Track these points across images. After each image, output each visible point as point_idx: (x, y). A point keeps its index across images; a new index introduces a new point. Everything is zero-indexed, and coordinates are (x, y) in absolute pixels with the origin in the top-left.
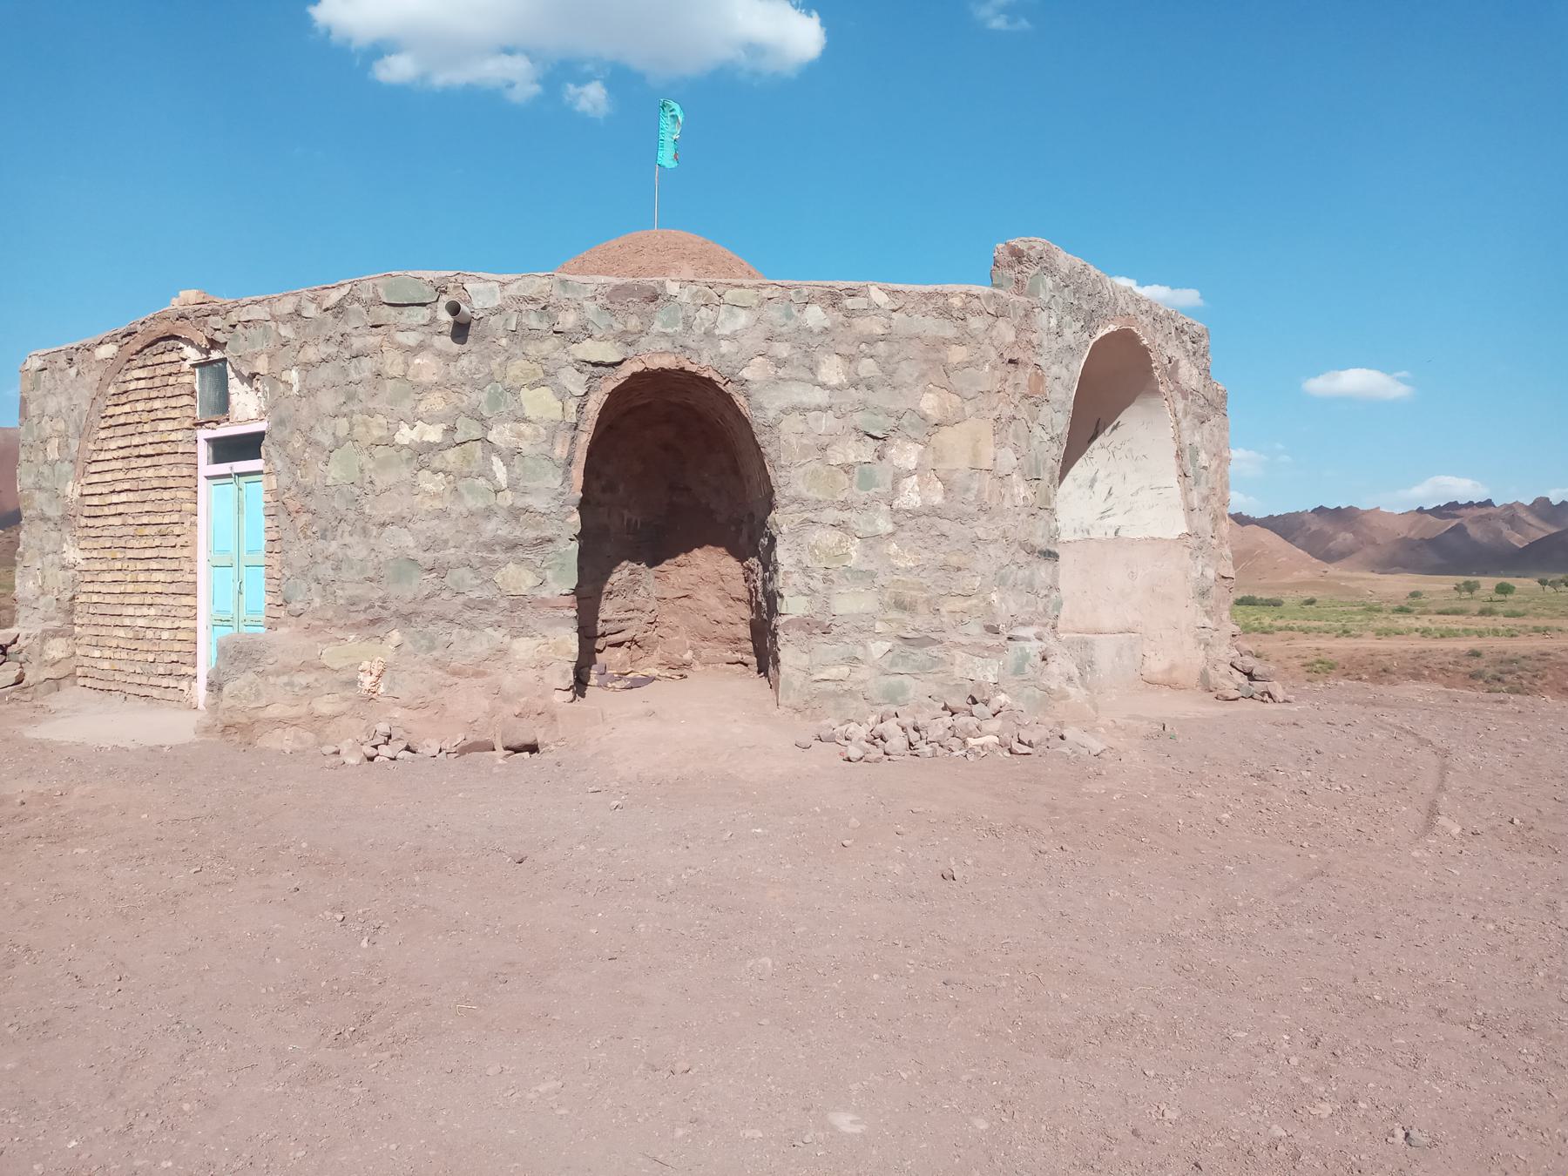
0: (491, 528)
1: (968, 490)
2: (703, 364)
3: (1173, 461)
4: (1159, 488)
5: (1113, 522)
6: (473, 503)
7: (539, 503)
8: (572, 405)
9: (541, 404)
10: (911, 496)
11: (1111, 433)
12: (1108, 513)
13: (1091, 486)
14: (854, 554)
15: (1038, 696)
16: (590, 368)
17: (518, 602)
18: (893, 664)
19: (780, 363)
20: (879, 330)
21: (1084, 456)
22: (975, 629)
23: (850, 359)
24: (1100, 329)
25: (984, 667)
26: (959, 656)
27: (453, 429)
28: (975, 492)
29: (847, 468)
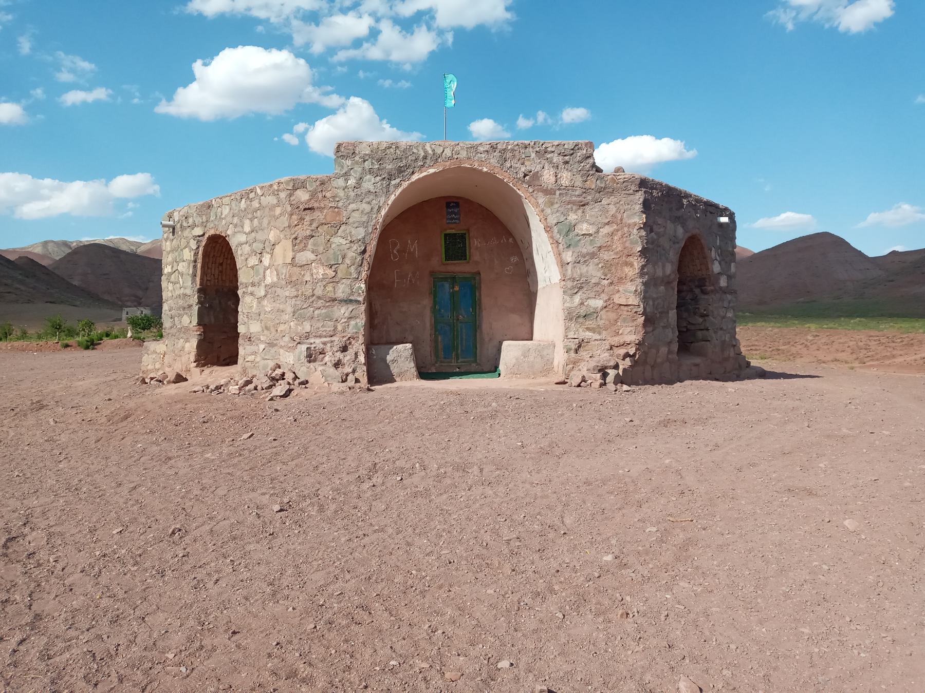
0: (181, 302)
1: (282, 274)
2: (220, 231)
6: (177, 293)
7: (188, 292)
8: (192, 253)
9: (188, 255)
10: (269, 280)
14: (255, 306)
15: (305, 371)
16: (198, 238)
17: (186, 329)
18: (265, 355)
19: (236, 226)
20: (258, 206)
22: (287, 339)
23: (251, 220)
25: (289, 356)
26: (282, 351)
27: (173, 267)
28: (284, 275)
29: (252, 267)
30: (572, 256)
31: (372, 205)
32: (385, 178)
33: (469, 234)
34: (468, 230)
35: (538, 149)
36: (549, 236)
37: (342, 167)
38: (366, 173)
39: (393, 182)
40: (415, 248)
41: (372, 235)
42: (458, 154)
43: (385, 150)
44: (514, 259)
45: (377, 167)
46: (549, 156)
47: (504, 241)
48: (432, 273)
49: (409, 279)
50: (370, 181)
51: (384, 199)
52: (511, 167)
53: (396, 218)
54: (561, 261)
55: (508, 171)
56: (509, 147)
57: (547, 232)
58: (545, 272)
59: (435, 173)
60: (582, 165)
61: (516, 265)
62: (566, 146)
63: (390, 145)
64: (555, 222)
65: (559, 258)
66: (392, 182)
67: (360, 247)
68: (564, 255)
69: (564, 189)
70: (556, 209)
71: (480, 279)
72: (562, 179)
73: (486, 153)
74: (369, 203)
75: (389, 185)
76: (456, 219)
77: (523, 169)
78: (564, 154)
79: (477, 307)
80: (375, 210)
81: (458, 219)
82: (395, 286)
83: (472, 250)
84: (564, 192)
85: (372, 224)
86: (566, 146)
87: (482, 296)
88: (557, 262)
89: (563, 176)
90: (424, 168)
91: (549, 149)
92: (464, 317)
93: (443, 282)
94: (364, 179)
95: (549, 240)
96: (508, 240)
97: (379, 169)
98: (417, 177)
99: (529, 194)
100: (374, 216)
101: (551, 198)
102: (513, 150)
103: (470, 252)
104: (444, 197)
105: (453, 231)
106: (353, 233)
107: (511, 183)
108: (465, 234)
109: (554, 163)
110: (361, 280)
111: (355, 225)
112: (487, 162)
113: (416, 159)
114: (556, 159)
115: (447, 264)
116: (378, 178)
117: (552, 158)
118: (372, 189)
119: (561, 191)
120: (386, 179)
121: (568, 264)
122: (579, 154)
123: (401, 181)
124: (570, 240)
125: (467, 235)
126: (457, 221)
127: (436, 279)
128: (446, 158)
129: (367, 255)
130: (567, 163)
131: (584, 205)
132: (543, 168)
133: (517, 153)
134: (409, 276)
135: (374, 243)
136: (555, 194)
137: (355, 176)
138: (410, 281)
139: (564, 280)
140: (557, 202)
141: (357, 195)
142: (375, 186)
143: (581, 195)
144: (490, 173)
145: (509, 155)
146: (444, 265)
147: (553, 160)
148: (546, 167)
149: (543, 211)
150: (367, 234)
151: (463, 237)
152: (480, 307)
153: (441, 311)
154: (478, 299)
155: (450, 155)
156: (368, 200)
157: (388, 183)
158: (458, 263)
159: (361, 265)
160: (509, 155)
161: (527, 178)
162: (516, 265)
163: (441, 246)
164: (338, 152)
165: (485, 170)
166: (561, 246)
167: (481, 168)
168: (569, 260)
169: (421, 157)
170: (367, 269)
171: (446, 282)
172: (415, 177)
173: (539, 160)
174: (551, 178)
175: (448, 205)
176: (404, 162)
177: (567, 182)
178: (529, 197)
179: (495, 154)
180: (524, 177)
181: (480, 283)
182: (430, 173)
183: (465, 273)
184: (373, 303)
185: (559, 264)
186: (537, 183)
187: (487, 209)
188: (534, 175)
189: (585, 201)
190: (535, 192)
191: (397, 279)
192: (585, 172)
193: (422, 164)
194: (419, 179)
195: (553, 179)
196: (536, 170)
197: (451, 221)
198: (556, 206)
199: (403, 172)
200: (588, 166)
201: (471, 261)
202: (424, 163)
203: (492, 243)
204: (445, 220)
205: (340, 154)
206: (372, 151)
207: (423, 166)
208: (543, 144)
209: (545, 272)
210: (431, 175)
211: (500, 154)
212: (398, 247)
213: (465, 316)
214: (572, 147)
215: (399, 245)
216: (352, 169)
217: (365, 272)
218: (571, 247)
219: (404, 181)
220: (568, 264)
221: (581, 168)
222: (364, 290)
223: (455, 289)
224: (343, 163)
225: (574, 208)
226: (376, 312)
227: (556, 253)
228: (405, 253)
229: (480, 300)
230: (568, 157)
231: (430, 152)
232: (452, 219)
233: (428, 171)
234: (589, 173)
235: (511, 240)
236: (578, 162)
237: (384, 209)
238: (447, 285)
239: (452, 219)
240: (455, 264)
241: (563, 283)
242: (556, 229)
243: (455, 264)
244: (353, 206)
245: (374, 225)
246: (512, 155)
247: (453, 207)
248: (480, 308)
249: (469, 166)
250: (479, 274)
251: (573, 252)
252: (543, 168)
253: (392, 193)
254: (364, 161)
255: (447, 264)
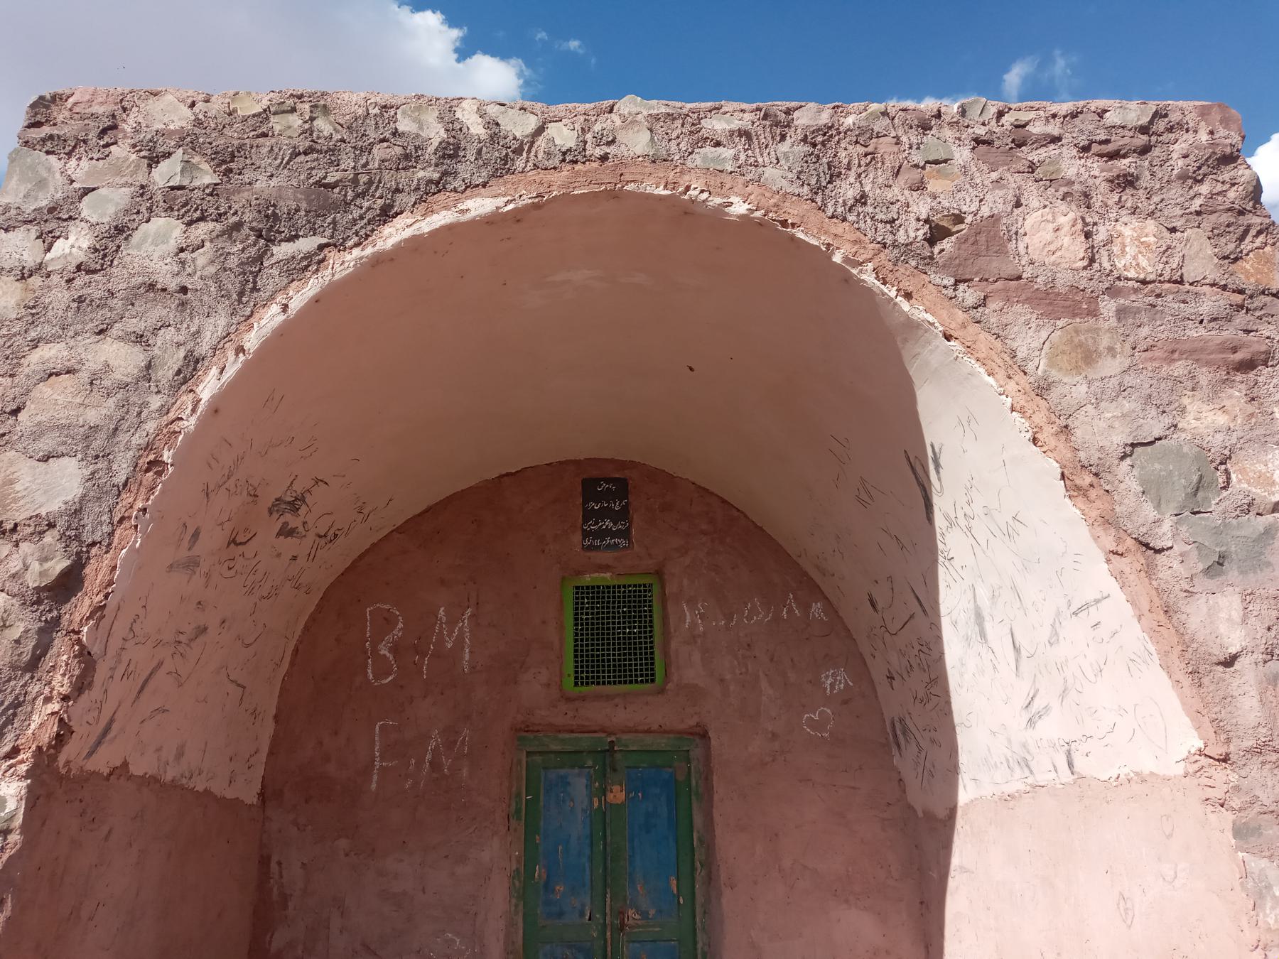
3: (1071, 511)
4: (1085, 607)
5: (1051, 729)
11: (939, 479)
12: (1038, 704)
13: (983, 634)
21: (941, 559)
24: (400, 222)
30: (1244, 620)
31: (156, 351)
32: (238, 226)
33: (663, 587)
34: (659, 573)
35: (981, 131)
36: (1094, 514)
37: (41, 184)
38: (150, 209)
39: (282, 251)
40: (460, 639)
41: (127, 498)
42: (609, 143)
43: (265, 115)
44: (835, 680)
45: (207, 177)
46: (1035, 156)
47: (790, 611)
48: (523, 731)
49: (429, 756)
50: (161, 238)
51: (222, 322)
52: (862, 199)
53: (399, 530)
54: (1185, 642)
55: (851, 218)
56: (849, 121)
57: (1076, 491)
58: (1031, 723)
59: (491, 221)
60: (1204, 189)
61: (845, 702)
62: (1112, 118)
63: (290, 102)
64: (1120, 438)
65: (1169, 634)
66: (275, 249)
67: (44, 560)
68: (1195, 615)
69: (1136, 291)
70: (1114, 381)
71: (708, 757)
72: (1116, 249)
73: (741, 143)
74: (140, 339)
75: (259, 259)
76: (614, 535)
77: (922, 207)
78: (1110, 148)
79: (700, 875)
80: (165, 374)
81: (625, 534)
82: (374, 786)
83: (674, 645)
84: (1141, 300)
85: (138, 439)
86: (1112, 118)
87: (718, 831)
88: (1164, 654)
89: (1120, 235)
90: (441, 197)
91: (1036, 129)
92: (645, 915)
93: (562, 772)
94: (137, 237)
95: (1096, 538)
96: (806, 607)
97: (214, 191)
98: (408, 233)
99: (961, 316)
100: (156, 402)
101: (1077, 332)
102: (864, 135)
103: (666, 654)
104: (577, 463)
105: (606, 578)
106: (18, 487)
107: (870, 266)
108: (648, 588)
109: (1070, 183)
110: (15, 751)
111: (47, 443)
112: (749, 177)
113: (407, 157)
114: (1071, 166)
115: (583, 698)
116: (202, 230)
117: (1054, 161)
118: (165, 273)
119: (1122, 301)
120: (246, 230)
121: (1229, 662)
122: (1178, 148)
123: (321, 247)
124: (1217, 531)
125: (656, 589)
126: (622, 542)
127: (538, 759)
128: (548, 154)
129: (82, 605)
130: (1126, 182)
131: (1247, 366)
132: (1018, 205)
133: (885, 146)
134: (432, 745)
135: (130, 540)
136: (1094, 313)
137: (93, 220)
138: (435, 765)
139: (1225, 759)
140: (1111, 350)
141: (81, 300)
142: (183, 263)
143: (1229, 319)
144: (761, 224)
145: (847, 152)
146: (569, 699)
147: (1058, 171)
148: (1033, 197)
149: (1042, 389)
150: (96, 489)
151: (642, 594)
152: (710, 873)
153: (554, 890)
154: (700, 839)
155: (571, 144)
156: (135, 325)
157: (252, 251)
158: (625, 695)
159: (33, 665)
160: (847, 152)
161: (947, 244)
162: (845, 702)
163: (561, 627)
164: (38, 124)
165: (739, 208)
166: (1171, 568)
167: (718, 201)
168: (1235, 640)
169: (431, 149)
170: (65, 690)
171: (576, 771)
172: (393, 234)
173: (994, 175)
174: (1066, 241)
175: (590, 488)
176: (347, 162)
177: (1144, 262)
178: (964, 326)
179: (784, 147)
180: (932, 240)
181: (707, 777)
182: (468, 216)
183: (649, 731)
184: (275, 859)
185: (1178, 665)
186: (996, 266)
187: (724, 501)
188: (977, 230)
189: (1255, 345)
190: (994, 305)
191: (382, 758)
192: (1226, 218)
193: (436, 176)
194: (415, 245)
195: (1075, 249)
196: (985, 211)
197: (597, 542)
198: (1110, 367)
199: (334, 207)
200: (1232, 194)
201: (670, 686)
202: (445, 174)
203: (749, 618)
204: (577, 538)
205: (46, 130)
206: (198, 123)
207: (438, 185)
208: (1000, 114)
209: (1031, 723)
210: (473, 222)
211: (808, 148)
212: (397, 633)
213: (652, 912)
214: (1145, 120)
215: (400, 625)
216: (87, 191)
217: (55, 706)
218: (1232, 573)
219: (340, 246)
220: (1229, 662)
221: (1198, 202)
222: (12, 817)
223: (610, 797)
224: (49, 170)
225: (1205, 377)
226: (285, 899)
227: (1145, 606)
228: (423, 655)
229: (709, 844)
230: (1126, 161)
231: (477, 128)
232: (602, 534)
233: (461, 207)
234: (1244, 220)
235: (817, 608)
236: (1183, 177)
237: (214, 371)
238: (579, 785)
239: (602, 534)
240: (609, 698)
241: (1221, 775)
242: (1127, 479)
243: (609, 698)
244: (51, 353)
245: (148, 447)
246: (862, 150)
247: (608, 495)
248: (710, 879)
249: (661, 191)
250: (702, 734)
251: (1248, 597)
252: (1018, 205)
253: (272, 298)
254: (154, 161)
255: (583, 698)
